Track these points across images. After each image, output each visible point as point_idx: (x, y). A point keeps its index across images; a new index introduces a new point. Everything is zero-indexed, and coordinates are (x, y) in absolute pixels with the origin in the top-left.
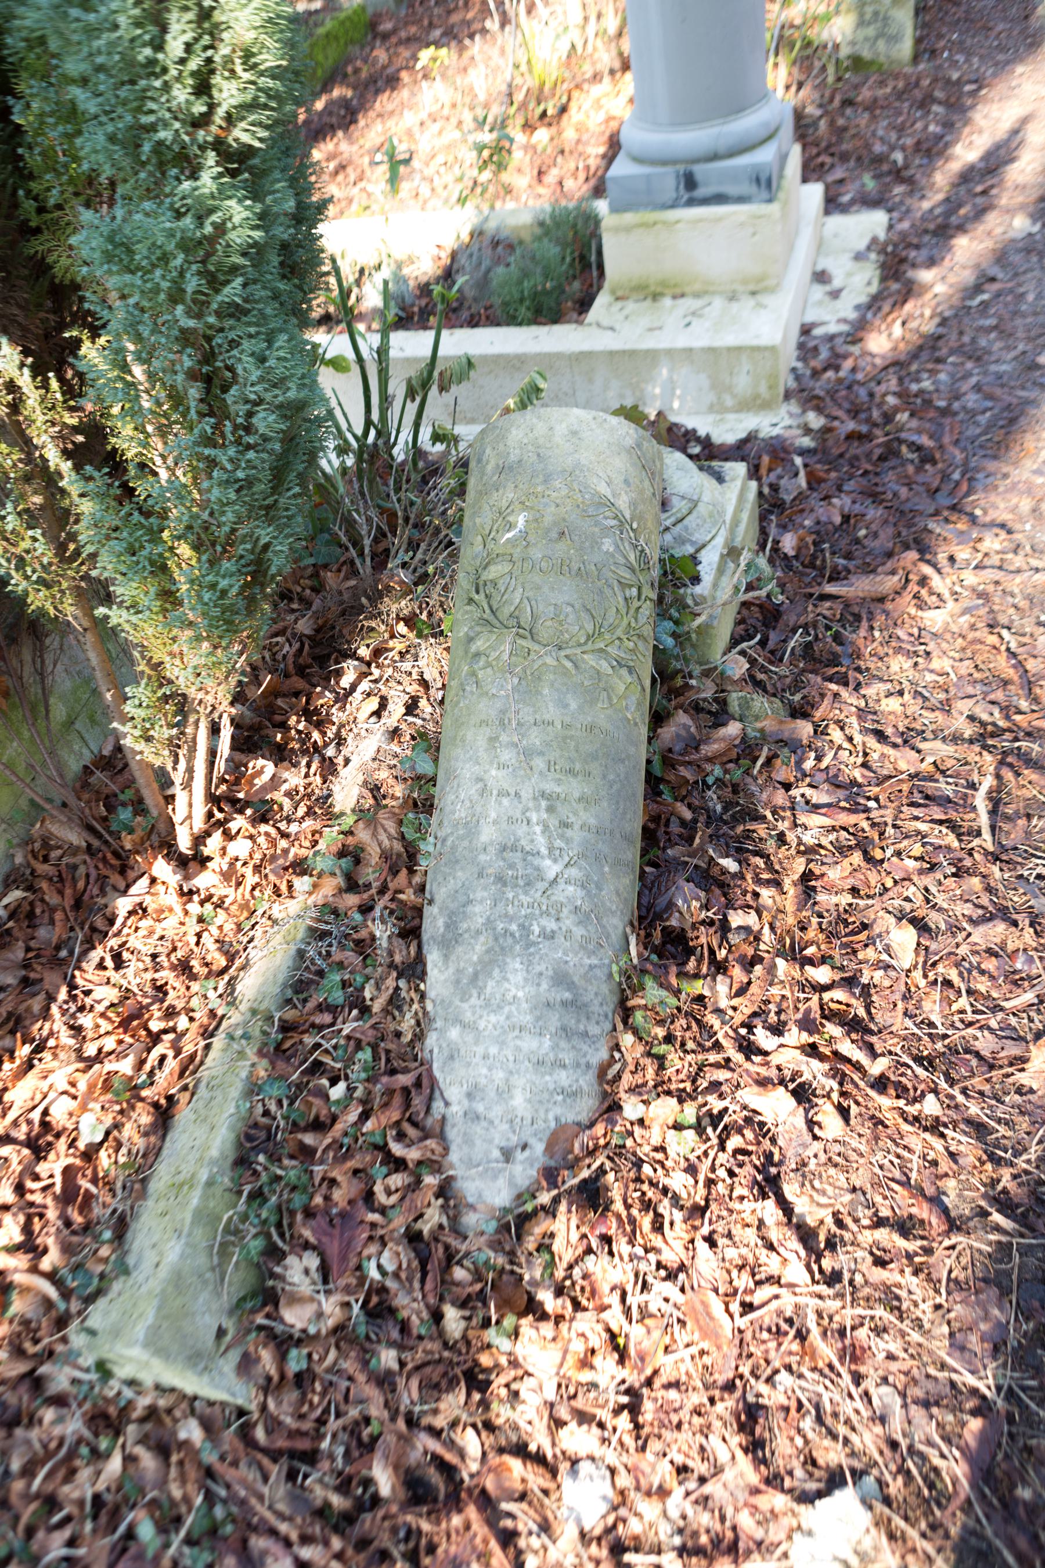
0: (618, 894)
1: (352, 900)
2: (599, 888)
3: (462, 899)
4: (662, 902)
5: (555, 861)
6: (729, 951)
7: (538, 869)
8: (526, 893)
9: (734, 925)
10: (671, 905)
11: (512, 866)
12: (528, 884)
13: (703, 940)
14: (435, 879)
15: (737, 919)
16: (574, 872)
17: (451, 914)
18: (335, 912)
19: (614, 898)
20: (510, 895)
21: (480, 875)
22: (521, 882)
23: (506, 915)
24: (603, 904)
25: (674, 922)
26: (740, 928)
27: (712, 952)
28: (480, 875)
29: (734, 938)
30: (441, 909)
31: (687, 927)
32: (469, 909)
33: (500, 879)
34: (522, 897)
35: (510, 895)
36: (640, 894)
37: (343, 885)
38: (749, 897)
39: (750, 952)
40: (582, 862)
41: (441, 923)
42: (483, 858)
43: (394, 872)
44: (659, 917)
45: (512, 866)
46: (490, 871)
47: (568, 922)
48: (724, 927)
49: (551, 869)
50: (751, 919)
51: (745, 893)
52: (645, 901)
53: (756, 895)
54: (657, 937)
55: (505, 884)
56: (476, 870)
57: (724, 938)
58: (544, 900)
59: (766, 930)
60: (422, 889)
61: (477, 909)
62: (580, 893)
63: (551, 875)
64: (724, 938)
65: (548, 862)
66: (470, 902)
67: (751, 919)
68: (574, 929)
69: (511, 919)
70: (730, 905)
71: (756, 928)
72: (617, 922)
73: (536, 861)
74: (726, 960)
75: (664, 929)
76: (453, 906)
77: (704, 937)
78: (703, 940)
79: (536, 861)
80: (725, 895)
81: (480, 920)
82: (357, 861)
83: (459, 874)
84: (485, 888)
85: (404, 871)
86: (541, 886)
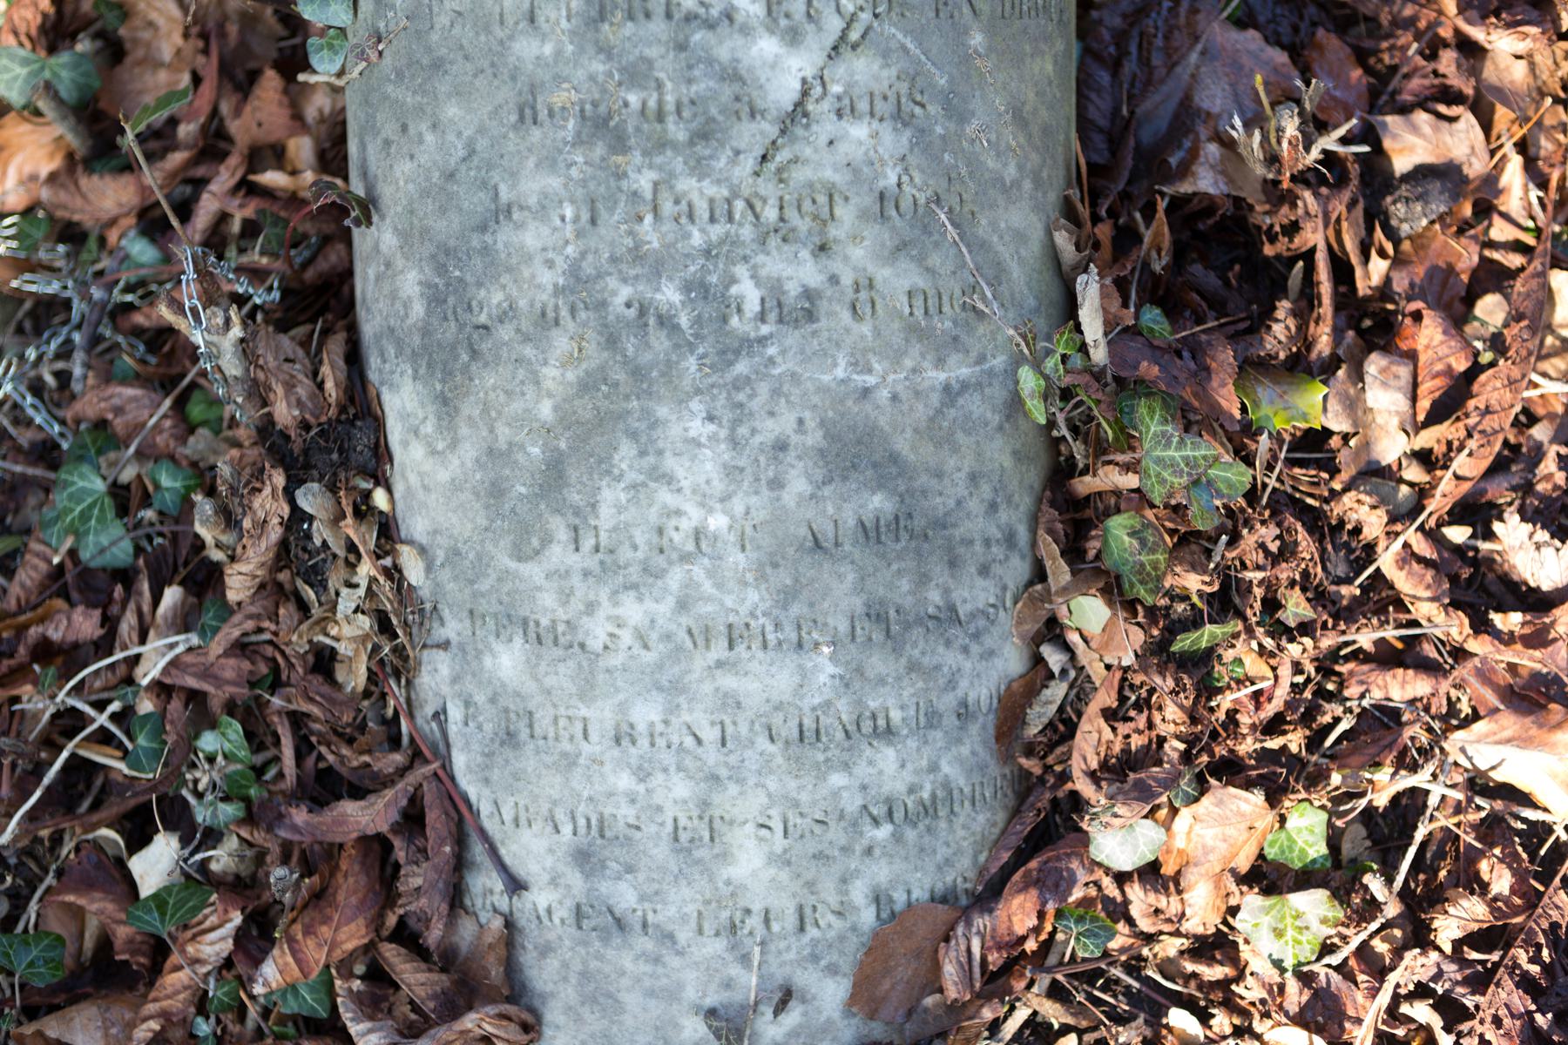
0: (1019, 118)
1: (109, 197)
2: (956, 111)
3: (475, 202)
4: (1158, 108)
5: (793, 37)
6: (1398, 261)
7: (733, 75)
8: (699, 168)
9: (1402, 164)
10: (1186, 117)
11: (637, 74)
12: (704, 134)
13: (1313, 236)
14: (370, 127)
15: (1411, 144)
16: (863, 70)
17: (443, 258)
18: (71, 234)
19: (1010, 137)
20: (644, 182)
21: (527, 114)
22: (677, 131)
23: (637, 254)
24: (973, 163)
25: (1205, 181)
26: (1422, 173)
27: (1342, 271)
28: (527, 114)
29: (1411, 217)
30: (404, 236)
31: (1253, 195)
32: (504, 237)
33: (601, 126)
34: (687, 184)
35: (644, 182)
36: (1084, 85)
37: (73, 141)
38: (1448, 61)
39: (1466, 256)
40: (891, 30)
41: (410, 283)
42: (527, 49)
43: (240, 80)
44: (1156, 165)
45: (637, 74)
46: (560, 97)
47: (859, 254)
48: (1373, 182)
49: (781, 67)
50: (1461, 141)
51: (1432, 50)
52: (1099, 111)
53: (1472, 51)
54: (1157, 235)
55: (619, 144)
56: (507, 94)
57: (1375, 216)
58: (767, 187)
59: (1513, 174)
60: (333, 157)
61: (532, 237)
62: (892, 142)
63: (783, 91)
64: (1375, 216)
65: (767, 46)
66: (502, 213)
67: (1461, 141)
68: (882, 274)
69: (656, 266)
70: (1384, 95)
71: (1477, 167)
72: (1022, 225)
73: (725, 48)
74: (1385, 291)
75: (1177, 203)
76: (445, 227)
77: (1317, 227)
78: (1313, 236)
79: (725, 48)
80: (1362, 57)
81: (547, 278)
82: (114, 51)
83: (452, 111)
84: (549, 162)
85: (271, 81)
86: (752, 135)
